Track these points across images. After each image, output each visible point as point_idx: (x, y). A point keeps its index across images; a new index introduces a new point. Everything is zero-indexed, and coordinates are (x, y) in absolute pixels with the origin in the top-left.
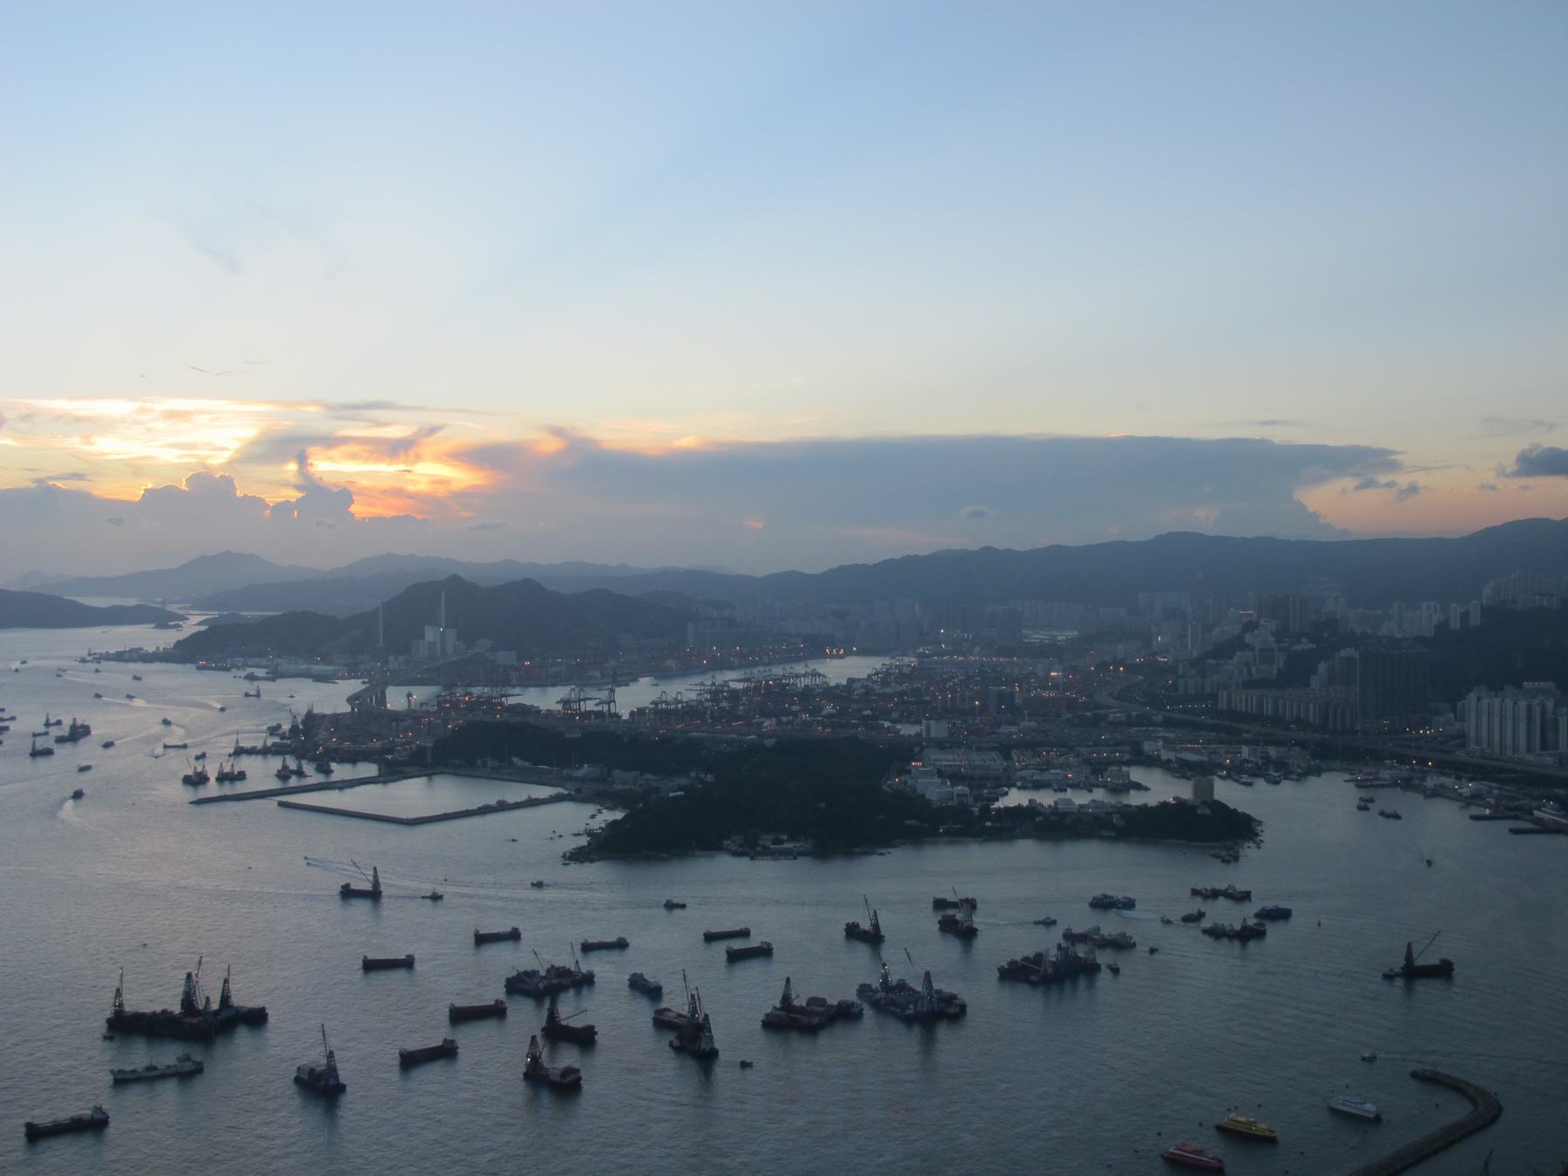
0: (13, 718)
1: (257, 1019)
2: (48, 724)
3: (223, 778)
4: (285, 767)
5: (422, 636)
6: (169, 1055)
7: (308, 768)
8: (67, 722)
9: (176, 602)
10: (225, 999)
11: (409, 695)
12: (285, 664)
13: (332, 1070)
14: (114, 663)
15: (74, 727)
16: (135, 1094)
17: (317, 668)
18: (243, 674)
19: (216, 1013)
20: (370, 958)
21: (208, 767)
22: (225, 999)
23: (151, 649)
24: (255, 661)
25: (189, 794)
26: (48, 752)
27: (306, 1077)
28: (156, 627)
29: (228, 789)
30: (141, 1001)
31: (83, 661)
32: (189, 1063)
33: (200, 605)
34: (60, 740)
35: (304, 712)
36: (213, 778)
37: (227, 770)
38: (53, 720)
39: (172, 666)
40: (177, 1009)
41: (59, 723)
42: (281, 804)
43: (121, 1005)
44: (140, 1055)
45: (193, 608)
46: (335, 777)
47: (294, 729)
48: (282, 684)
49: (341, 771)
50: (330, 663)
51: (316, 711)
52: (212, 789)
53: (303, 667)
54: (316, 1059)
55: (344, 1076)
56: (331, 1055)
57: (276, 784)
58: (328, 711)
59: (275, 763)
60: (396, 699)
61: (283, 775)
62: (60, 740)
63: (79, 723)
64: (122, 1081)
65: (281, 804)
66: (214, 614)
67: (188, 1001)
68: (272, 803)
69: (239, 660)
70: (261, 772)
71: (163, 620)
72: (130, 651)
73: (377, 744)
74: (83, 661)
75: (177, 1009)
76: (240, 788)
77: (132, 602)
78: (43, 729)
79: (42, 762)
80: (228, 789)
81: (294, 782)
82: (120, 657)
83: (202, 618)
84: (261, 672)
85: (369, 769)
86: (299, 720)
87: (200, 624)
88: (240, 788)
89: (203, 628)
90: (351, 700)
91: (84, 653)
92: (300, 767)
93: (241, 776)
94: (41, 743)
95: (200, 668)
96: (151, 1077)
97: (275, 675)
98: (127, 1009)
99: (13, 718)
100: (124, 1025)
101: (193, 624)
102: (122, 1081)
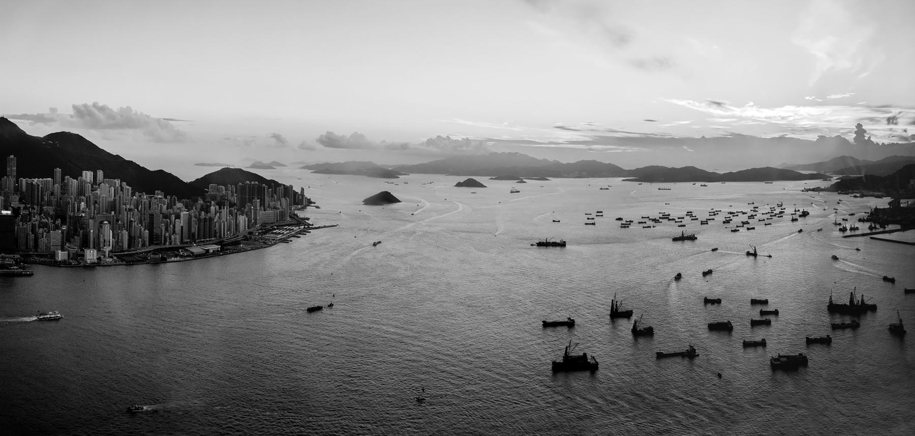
0: (785, 209)
1: (873, 308)
2: (795, 211)
3: (851, 229)
4: (871, 226)
5: (910, 183)
6: (848, 320)
7: (878, 226)
8: (801, 210)
9: (828, 172)
10: (862, 300)
11: (908, 202)
12: (865, 192)
13: (901, 326)
14: (812, 192)
15: (804, 212)
16: (839, 333)
17: (876, 193)
18: (853, 195)
19: (860, 305)
20: (907, 289)
21: (847, 226)
22: (862, 300)
23: (823, 188)
24: (856, 191)
25: (841, 234)
26: (796, 220)
27: (892, 327)
28: (823, 180)
29: (853, 233)
30: (838, 301)
31: (803, 191)
32: (855, 323)
33: (837, 173)
34: (800, 216)
35: (875, 207)
36: (848, 228)
37: (853, 226)
38: (797, 210)
39: (830, 193)
40: (848, 304)
41: (799, 211)
42: (871, 238)
43: (832, 301)
44: (838, 320)
45: (833, 174)
46: (887, 229)
47: (871, 213)
48: (865, 199)
49: (890, 227)
50: (880, 192)
51: (878, 207)
52: (848, 233)
53: (872, 193)
54: (895, 321)
55: (905, 328)
56: (901, 321)
57: (868, 231)
58: (882, 207)
59: (868, 225)
60: (904, 203)
61: (871, 228)
62: (800, 216)
63: (805, 210)
64: (835, 327)
65: (871, 238)
66: (841, 176)
67: (852, 301)
68: (868, 238)
69: (850, 191)
70: (864, 227)
71: (825, 178)
72: (817, 188)
73: (899, 218)
74: (803, 191)
75: (848, 304)
76: (857, 232)
77: (815, 172)
78: (794, 213)
79: (795, 223)
80: (853, 233)
81: (874, 231)
82: (813, 190)
83: (837, 177)
84: (858, 195)
85: (898, 227)
86: (873, 210)
87: (837, 179)
88: (857, 232)
89: (839, 181)
90: (889, 204)
91: (803, 189)
92: (875, 226)
93: (857, 229)
94: (794, 217)
95: (839, 193)
96: (843, 327)
97: (862, 196)
98: (834, 303)
99: (785, 209)
100: (833, 308)
101: (835, 180)
102: (835, 327)
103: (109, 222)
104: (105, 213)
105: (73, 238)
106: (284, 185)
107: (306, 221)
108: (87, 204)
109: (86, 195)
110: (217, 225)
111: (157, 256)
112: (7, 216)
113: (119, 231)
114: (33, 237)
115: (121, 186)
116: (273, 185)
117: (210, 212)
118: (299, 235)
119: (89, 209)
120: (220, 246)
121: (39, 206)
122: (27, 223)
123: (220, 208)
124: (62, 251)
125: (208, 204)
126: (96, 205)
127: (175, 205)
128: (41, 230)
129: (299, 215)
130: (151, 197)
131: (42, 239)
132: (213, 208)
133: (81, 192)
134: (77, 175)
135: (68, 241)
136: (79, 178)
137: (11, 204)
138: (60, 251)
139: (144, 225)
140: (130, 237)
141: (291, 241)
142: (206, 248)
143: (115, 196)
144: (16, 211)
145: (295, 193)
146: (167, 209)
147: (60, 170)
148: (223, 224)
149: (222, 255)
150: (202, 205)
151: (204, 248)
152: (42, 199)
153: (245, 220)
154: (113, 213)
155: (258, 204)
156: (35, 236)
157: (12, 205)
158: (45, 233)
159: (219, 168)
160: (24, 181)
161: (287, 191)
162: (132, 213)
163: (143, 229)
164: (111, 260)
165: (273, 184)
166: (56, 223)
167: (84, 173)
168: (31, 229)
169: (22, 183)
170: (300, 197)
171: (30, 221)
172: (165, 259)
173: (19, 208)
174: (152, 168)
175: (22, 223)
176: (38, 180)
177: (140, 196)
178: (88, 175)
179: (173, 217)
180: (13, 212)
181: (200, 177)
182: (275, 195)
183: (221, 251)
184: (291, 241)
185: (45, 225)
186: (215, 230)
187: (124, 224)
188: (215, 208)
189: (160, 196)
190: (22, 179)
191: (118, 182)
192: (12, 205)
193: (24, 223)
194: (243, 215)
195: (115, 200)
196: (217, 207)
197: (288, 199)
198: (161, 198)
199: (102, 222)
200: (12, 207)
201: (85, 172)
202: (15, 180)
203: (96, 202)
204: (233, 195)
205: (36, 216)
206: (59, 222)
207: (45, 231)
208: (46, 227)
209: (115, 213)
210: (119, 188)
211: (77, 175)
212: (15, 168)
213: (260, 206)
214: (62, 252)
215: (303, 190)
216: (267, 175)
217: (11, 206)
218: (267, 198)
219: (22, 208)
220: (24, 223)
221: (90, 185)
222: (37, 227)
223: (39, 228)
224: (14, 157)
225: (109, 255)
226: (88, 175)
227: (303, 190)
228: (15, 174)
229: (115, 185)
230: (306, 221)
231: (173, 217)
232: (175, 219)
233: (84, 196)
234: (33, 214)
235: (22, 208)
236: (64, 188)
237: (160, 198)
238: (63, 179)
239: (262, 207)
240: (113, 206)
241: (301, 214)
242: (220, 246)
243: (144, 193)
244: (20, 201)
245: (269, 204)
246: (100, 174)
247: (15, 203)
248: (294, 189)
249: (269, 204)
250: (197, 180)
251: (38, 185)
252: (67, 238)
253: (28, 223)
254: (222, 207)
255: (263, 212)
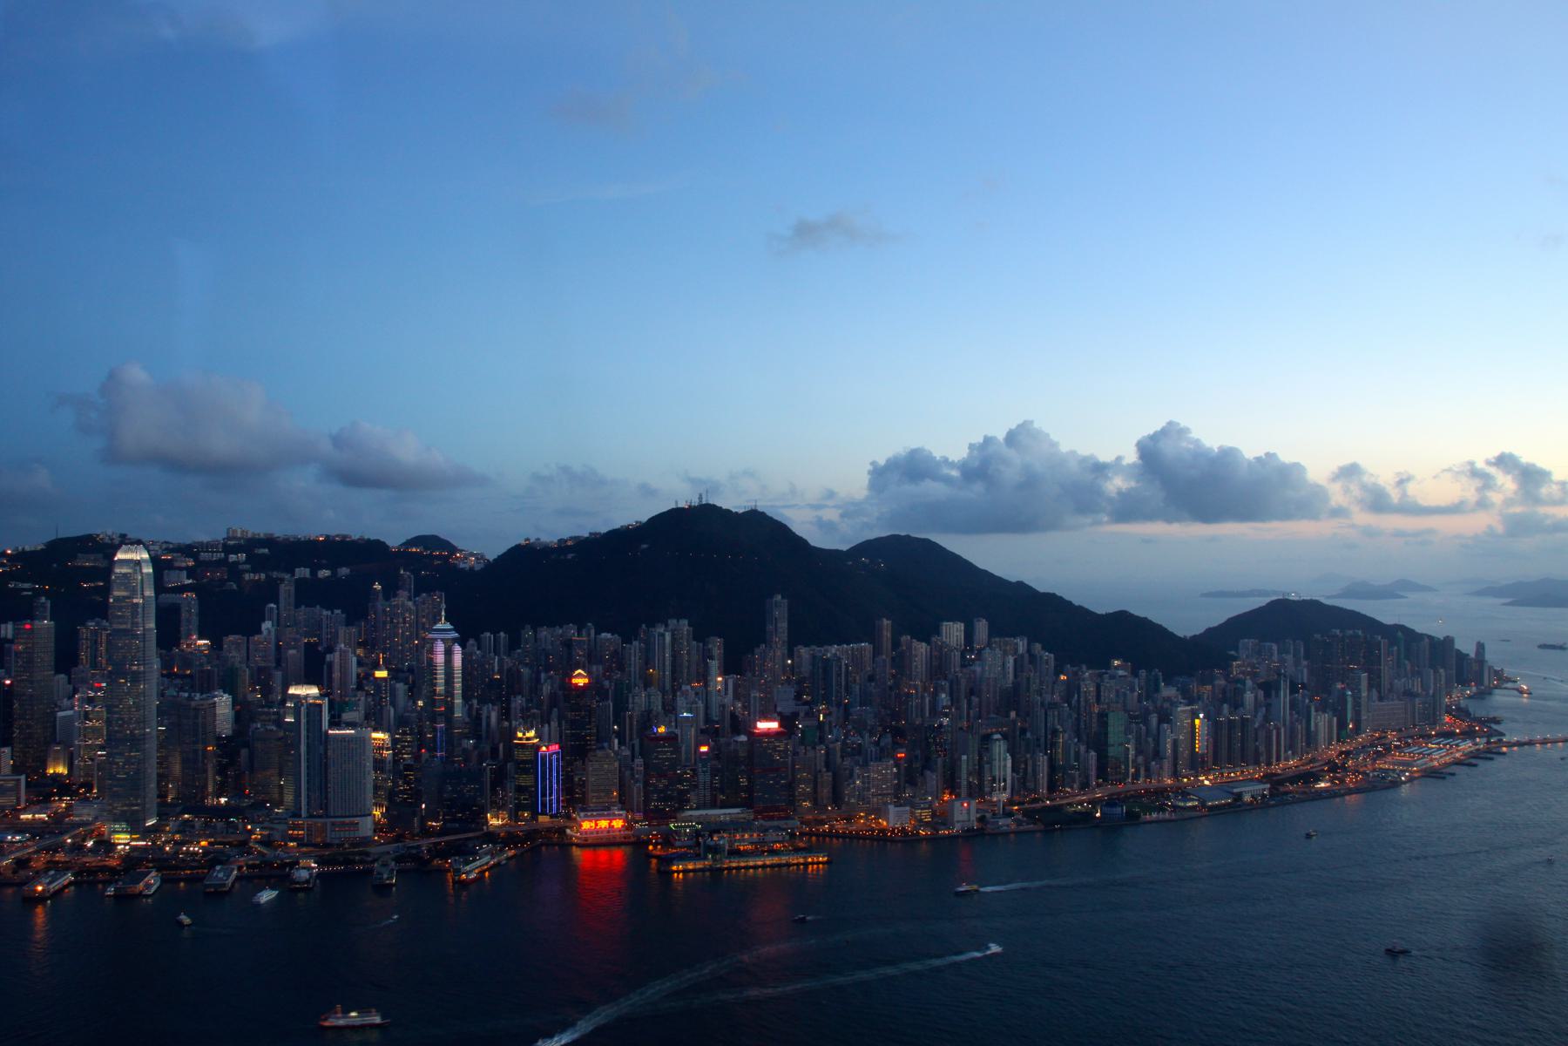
103: (1005, 736)
104: (993, 715)
105: (922, 774)
106: (1430, 637)
107: (1495, 727)
108: (952, 700)
109: (950, 677)
110: (1262, 734)
111: (1119, 809)
112: (768, 734)
113: (1028, 756)
114: (830, 779)
115: (1029, 651)
116: (1402, 637)
117: (1242, 705)
118: (1473, 761)
119: (957, 709)
120: (1268, 786)
121: (842, 707)
122: (814, 748)
123: (1267, 695)
124: (896, 806)
125: (1239, 685)
126: (973, 698)
127: (1157, 690)
128: (847, 762)
129: (1471, 710)
130: (1100, 675)
131: (851, 781)
132: (1249, 697)
133: (938, 668)
134: (927, 632)
135: (911, 781)
136: (934, 639)
137: (776, 706)
138: (891, 808)
139: (1085, 738)
140: (1053, 768)
141: (1453, 774)
142: (1235, 790)
143: (1016, 676)
144: (787, 721)
145: (1461, 657)
146: (1140, 701)
147: (889, 622)
148: (1274, 732)
149: (1273, 806)
150: (1224, 692)
151: (1230, 790)
152: (848, 690)
153: (1330, 722)
154: (1013, 714)
155: (1364, 684)
156: (835, 776)
157: (779, 709)
158: (857, 770)
159: (1262, 602)
160: (804, 651)
161: (1441, 650)
162: (1056, 713)
163: (1083, 748)
164: (1009, 821)
165: (1400, 634)
166: (882, 744)
167: (944, 628)
168: (823, 758)
169: (800, 656)
170: (1475, 667)
171: (822, 740)
172: (1137, 816)
173: (795, 716)
174: (1101, 609)
175: (803, 747)
176: (838, 650)
177: (1076, 674)
178: (953, 632)
179: (1154, 719)
180: (780, 726)
181: (1216, 625)
182: (1407, 662)
183: (1271, 794)
184: (1453, 774)
185: (859, 750)
186: (1257, 748)
187: (1038, 740)
188: (1256, 698)
189: (1121, 673)
190: (799, 647)
191: (1021, 644)
192: (779, 709)
193: (808, 748)
194: (1324, 712)
195: (1016, 686)
196: (1261, 693)
197: (1442, 671)
198: (1125, 676)
199: (987, 738)
200: (780, 714)
201: (945, 623)
202: (786, 651)
203: (972, 692)
204: (1297, 663)
205: (835, 731)
206: (888, 739)
207: (857, 763)
208: (859, 753)
209: (1017, 715)
210: (1026, 656)
211: (927, 632)
212: (785, 625)
213: (1370, 687)
214: (897, 809)
215: (1480, 647)
216: (1386, 613)
217: (775, 711)
218: (1386, 670)
219: (802, 714)
220: (808, 748)
221: (958, 654)
222: (839, 754)
223: (842, 757)
224: (783, 597)
225: (1003, 808)
226: (953, 632)
227: (1480, 647)
228: (785, 636)
229: (1016, 650)
230: (1495, 727)
231: (1154, 719)
232: (1160, 722)
233: (945, 679)
234: (827, 728)
235: (802, 714)
236: (901, 662)
237: (1121, 676)
238: (896, 644)
239: (1374, 690)
240: (1013, 698)
241: (1477, 709)
242: (1268, 786)
243: (1084, 667)
244: (798, 697)
245: (1391, 684)
246: (982, 627)
247: (785, 699)
248: (1457, 646)
249: (1391, 684)
250: (1210, 631)
251: (839, 659)
252: (911, 777)
253: (818, 748)
254: (1273, 693)
255: (1377, 703)
